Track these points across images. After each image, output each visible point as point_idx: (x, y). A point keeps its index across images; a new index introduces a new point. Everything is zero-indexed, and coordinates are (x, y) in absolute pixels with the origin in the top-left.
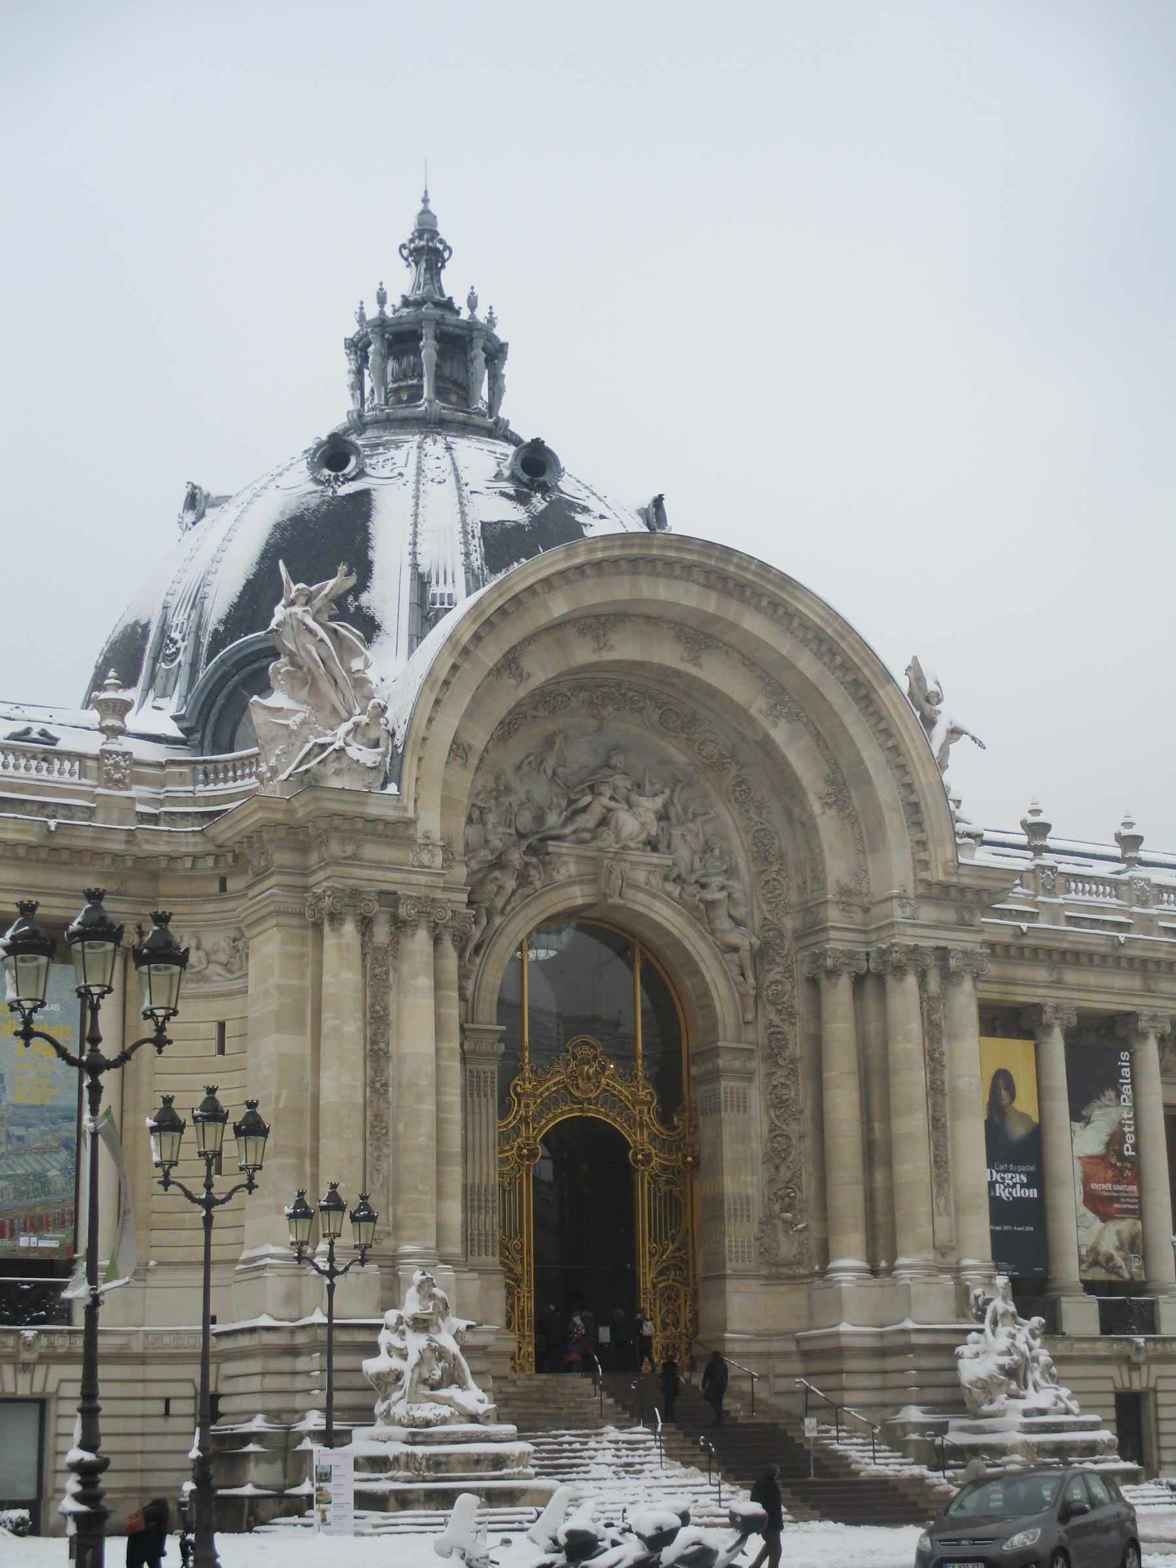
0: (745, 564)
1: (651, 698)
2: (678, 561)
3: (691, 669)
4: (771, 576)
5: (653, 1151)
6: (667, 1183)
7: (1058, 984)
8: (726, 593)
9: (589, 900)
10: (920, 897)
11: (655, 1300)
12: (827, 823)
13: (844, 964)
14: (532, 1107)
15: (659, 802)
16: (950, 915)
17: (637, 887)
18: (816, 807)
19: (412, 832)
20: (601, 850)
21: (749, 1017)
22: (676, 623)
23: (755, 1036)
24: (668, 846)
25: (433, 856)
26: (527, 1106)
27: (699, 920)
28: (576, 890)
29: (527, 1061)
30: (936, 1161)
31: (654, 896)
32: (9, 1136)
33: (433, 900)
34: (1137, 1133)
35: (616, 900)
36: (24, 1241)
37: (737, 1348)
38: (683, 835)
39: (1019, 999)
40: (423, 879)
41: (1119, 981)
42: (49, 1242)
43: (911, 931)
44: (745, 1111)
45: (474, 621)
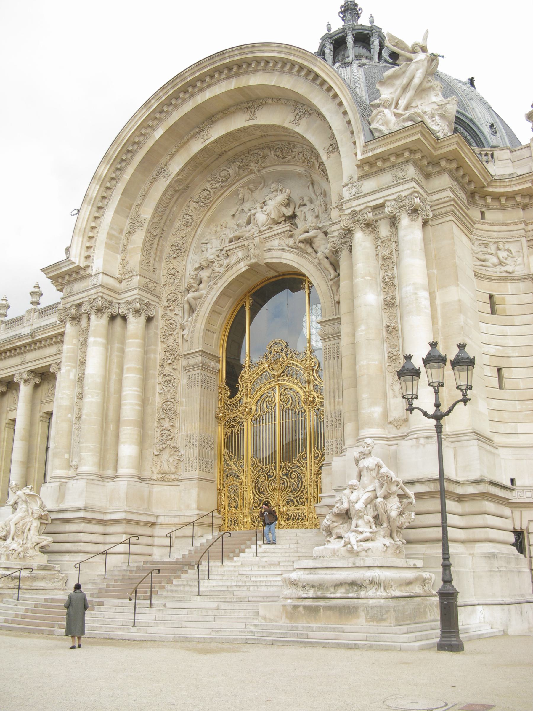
0: (232, 54)
1: (267, 147)
2: (205, 74)
4: (246, 50)
5: (316, 395)
8: (237, 75)
10: (361, 178)
11: (317, 486)
13: (341, 244)
14: (249, 386)
17: (272, 250)
19: (89, 271)
20: (248, 238)
22: (238, 105)
26: (247, 386)
27: (307, 253)
28: (242, 264)
29: (247, 362)
30: (389, 358)
31: (282, 250)
33: (95, 299)
43: (355, 203)
44: (338, 357)
45: (108, 163)
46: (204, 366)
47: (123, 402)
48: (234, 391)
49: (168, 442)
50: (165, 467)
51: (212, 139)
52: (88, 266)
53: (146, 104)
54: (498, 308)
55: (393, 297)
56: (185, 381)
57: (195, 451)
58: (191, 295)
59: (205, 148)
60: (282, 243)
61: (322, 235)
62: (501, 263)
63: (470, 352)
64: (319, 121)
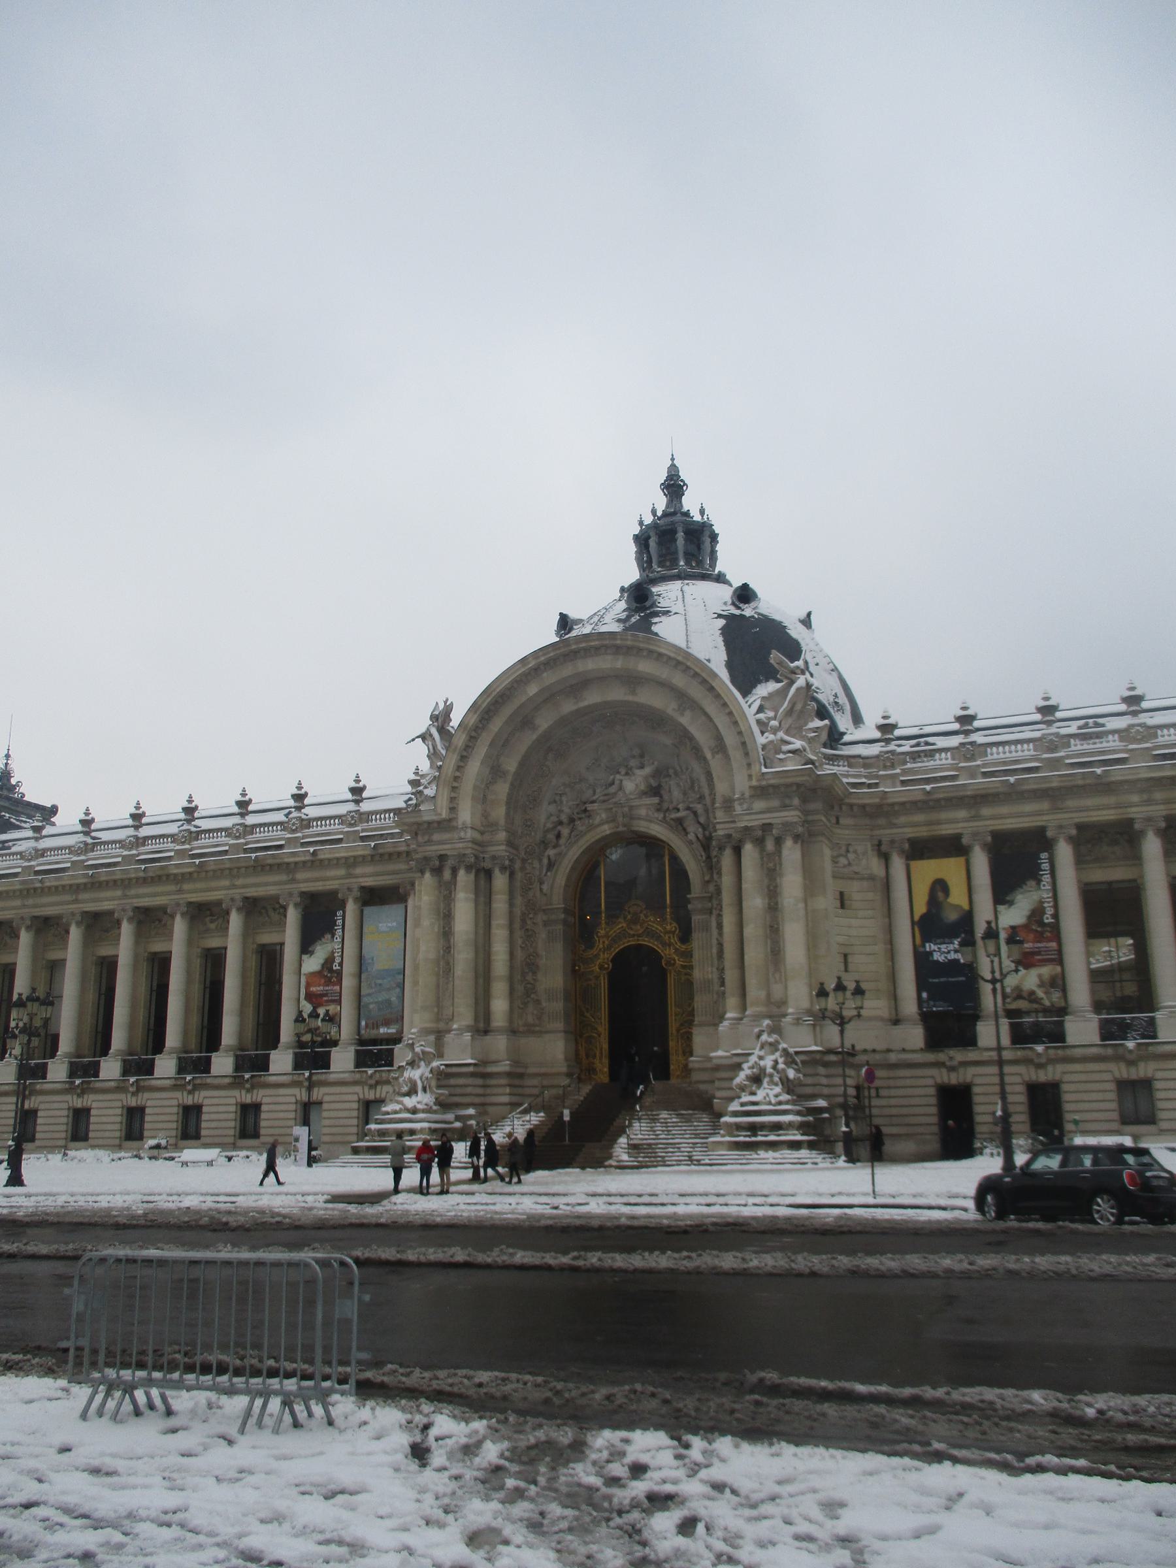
2: (591, 647)
3: (630, 698)
6: (686, 974)
7: (976, 817)
9: (612, 831)
12: (715, 763)
14: (607, 942)
15: (648, 770)
16: (775, 803)
18: (709, 755)
19: (454, 824)
20: (615, 803)
21: (707, 878)
23: (711, 888)
24: (670, 791)
25: (466, 833)
28: (606, 827)
30: (772, 952)
31: (650, 821)
32: (376, 984)
34: (1056, 906)
35: (621, 829)
36: (382, 1030)
37: (696, 1066)
38: (678, 785)
39: (944, 832)
40: (461, 845)
41: (1028, 808)
42: (392, 1030)
45: (475, 712)
46: (565, 922)
47: (493, 958)
48: (590, 944)
49: (532, 996)
50: (530, 1019)
51: (586, 703)
52: (454, 818)
53: (523, 661)
54: (847, 903)
55: (777, 903)
56: (543, 935)
57: (558, 1006)
58: (551, 852)
59: (577, 711)
60: (650, 813)
61: (692, 816)
62: (850, 864)
63: (864, 986)
64: (703, 718)
